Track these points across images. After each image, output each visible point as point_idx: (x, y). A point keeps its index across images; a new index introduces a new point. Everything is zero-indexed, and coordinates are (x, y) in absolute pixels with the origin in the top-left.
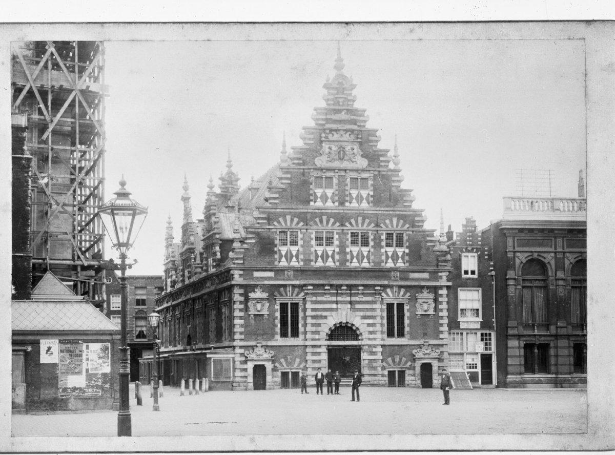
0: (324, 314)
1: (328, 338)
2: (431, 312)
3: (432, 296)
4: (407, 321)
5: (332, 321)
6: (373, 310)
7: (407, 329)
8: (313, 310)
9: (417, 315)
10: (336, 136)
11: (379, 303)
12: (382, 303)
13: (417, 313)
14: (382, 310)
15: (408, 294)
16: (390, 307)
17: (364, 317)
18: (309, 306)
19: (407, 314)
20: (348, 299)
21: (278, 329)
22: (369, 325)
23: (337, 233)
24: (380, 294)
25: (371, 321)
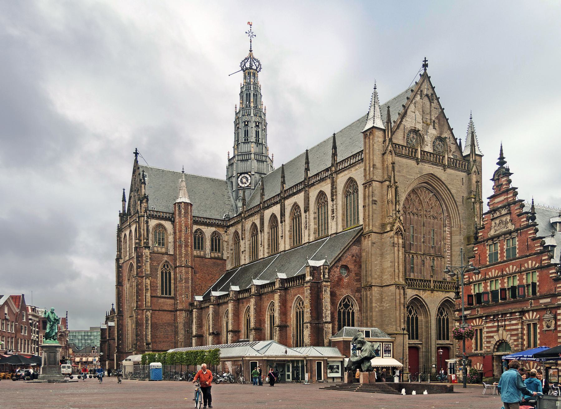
0: (492, 334)
1: (495, 350)
2: (552, 327)
3: (551, 316)
4: (538, 336)
5: (497, 338)
6: (517, 329)
7: (538, 342)
8: (488, 332)
9: (543, 331)
10: (498, 214)
11: (520, 324)
12: (522, 323)
13: (543, 330)
14: (523, 329)
15: (538, 316)
16: (529, 325)
17: (512, 335)
18: (485, 330)
19: (538, 331)
20: (503, 323)
21: (473, 346)
22: (515, 340)
23: (500, 280)
24: (522, 318)
25: (515, 338)
